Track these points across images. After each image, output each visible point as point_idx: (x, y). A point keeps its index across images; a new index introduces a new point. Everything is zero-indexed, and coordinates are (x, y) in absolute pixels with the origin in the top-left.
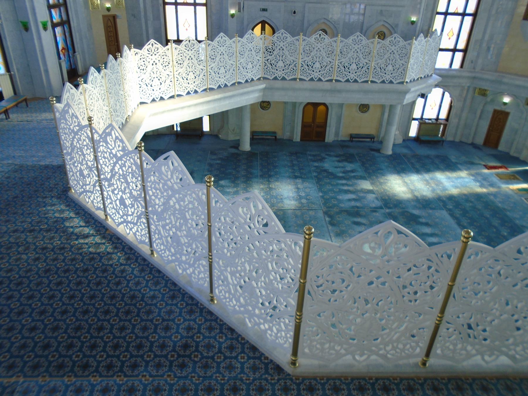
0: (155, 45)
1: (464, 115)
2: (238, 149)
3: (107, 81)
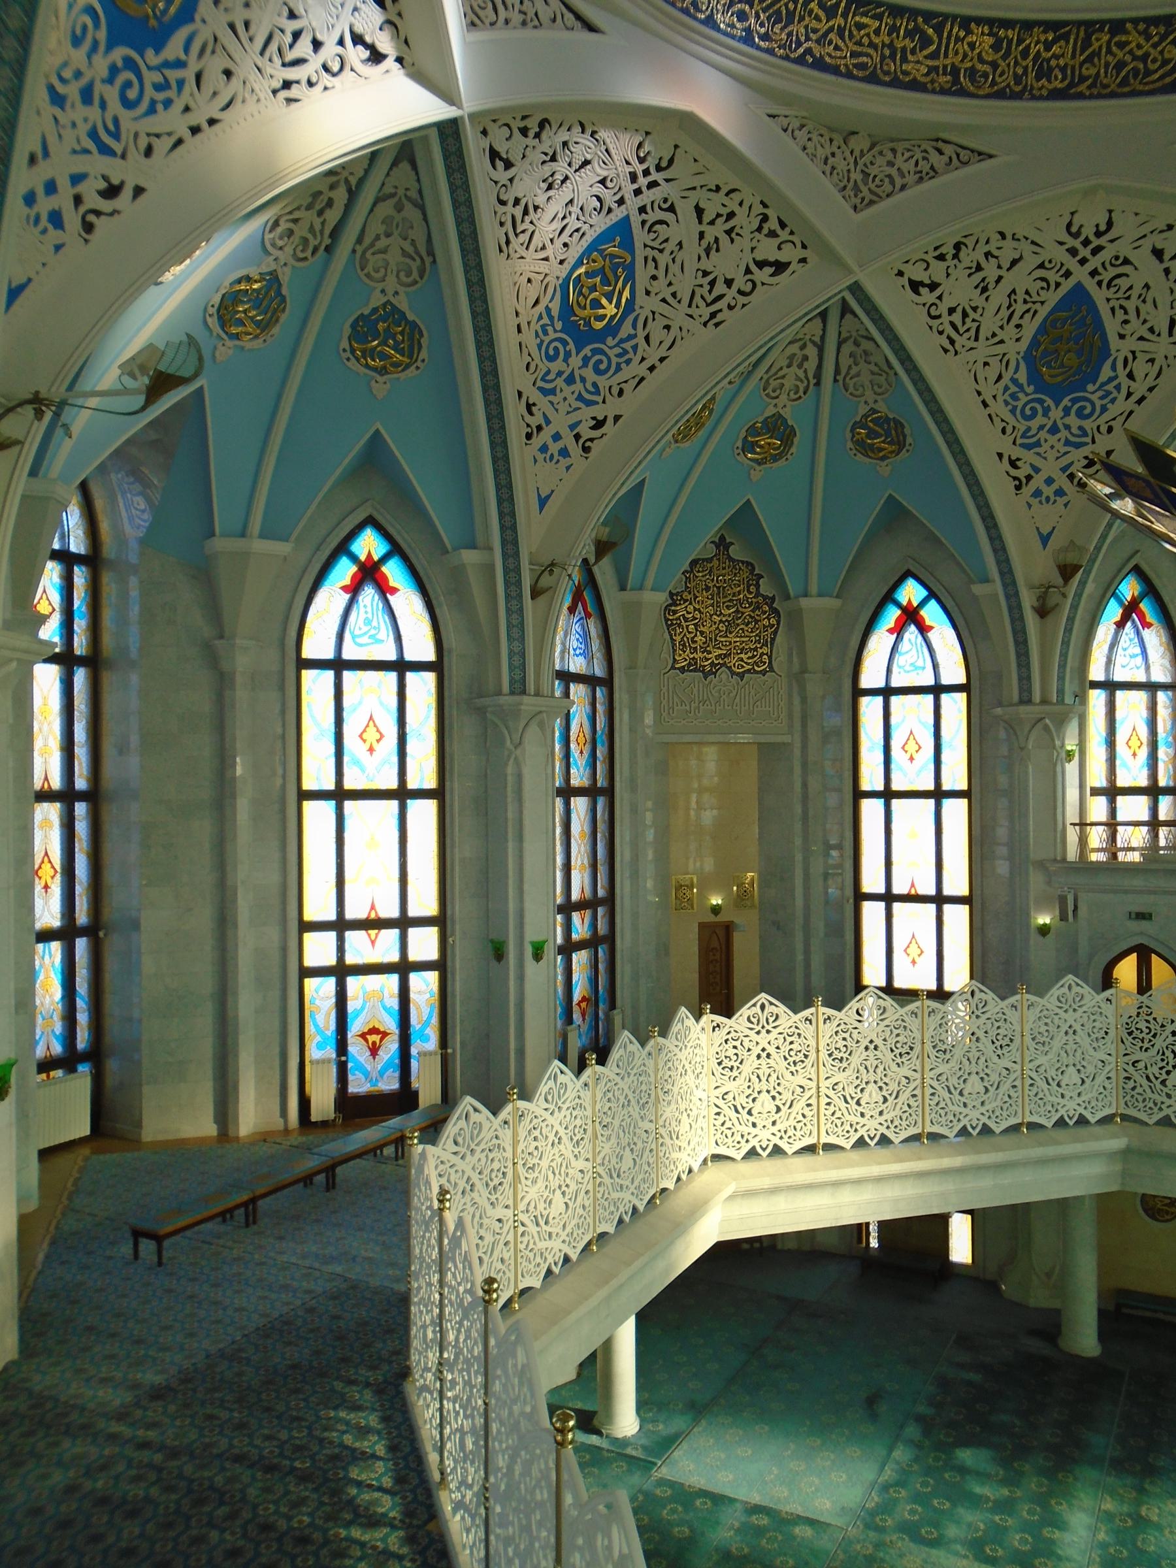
0: (769, 1009)
2: (1056, 1346)
3: (599, 1095)
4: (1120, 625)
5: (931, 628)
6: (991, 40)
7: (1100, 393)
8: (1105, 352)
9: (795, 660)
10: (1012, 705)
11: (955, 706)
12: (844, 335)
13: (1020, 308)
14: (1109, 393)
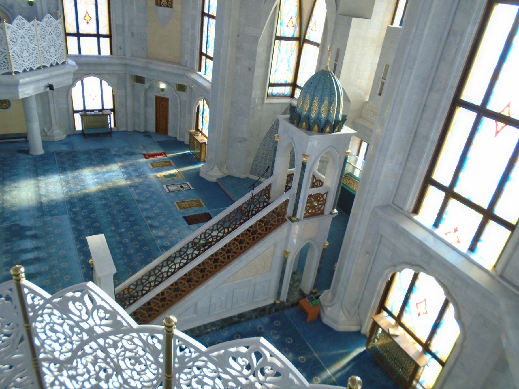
1: (129, 103)
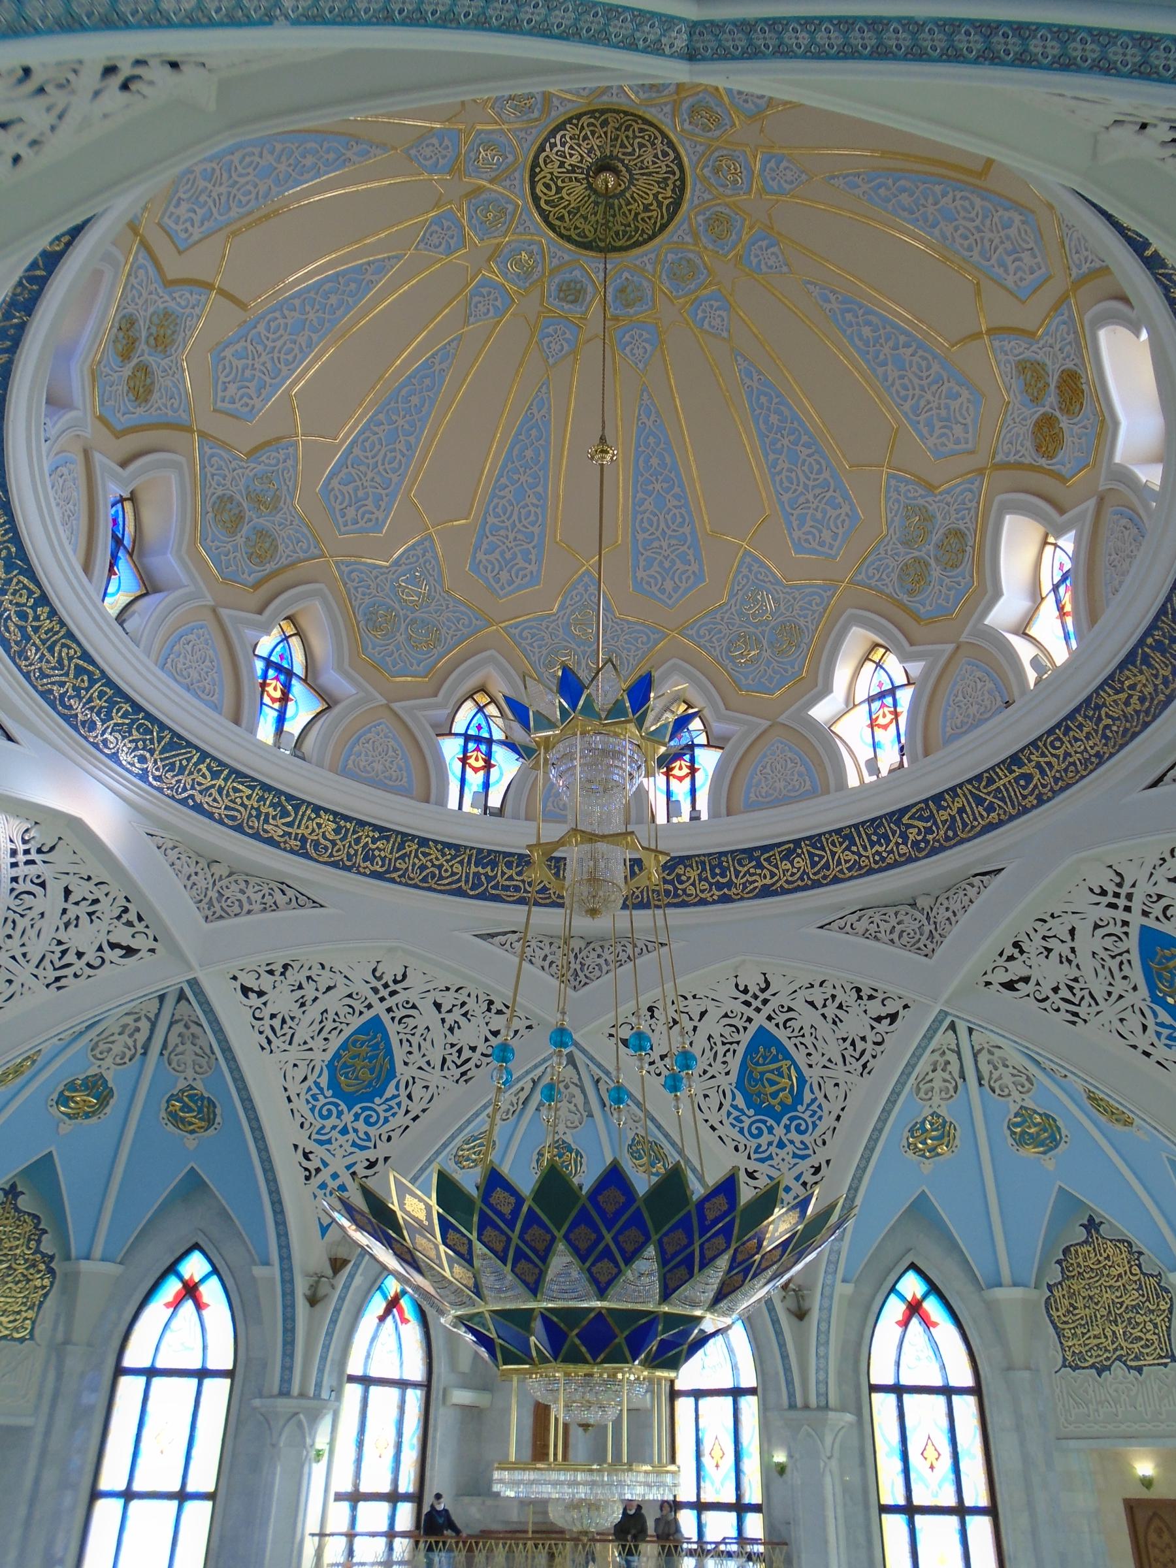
4: (382, 1319)
5: (207, 1305)
6: (334, 826)
7: (385, 1107)
8: (392, 1073)
9: (61, 1328)
10: (272, 1396)
11: (217, 1391)
12: (177, 1017)
13: (329, 1025)
14: (391, 1108)
